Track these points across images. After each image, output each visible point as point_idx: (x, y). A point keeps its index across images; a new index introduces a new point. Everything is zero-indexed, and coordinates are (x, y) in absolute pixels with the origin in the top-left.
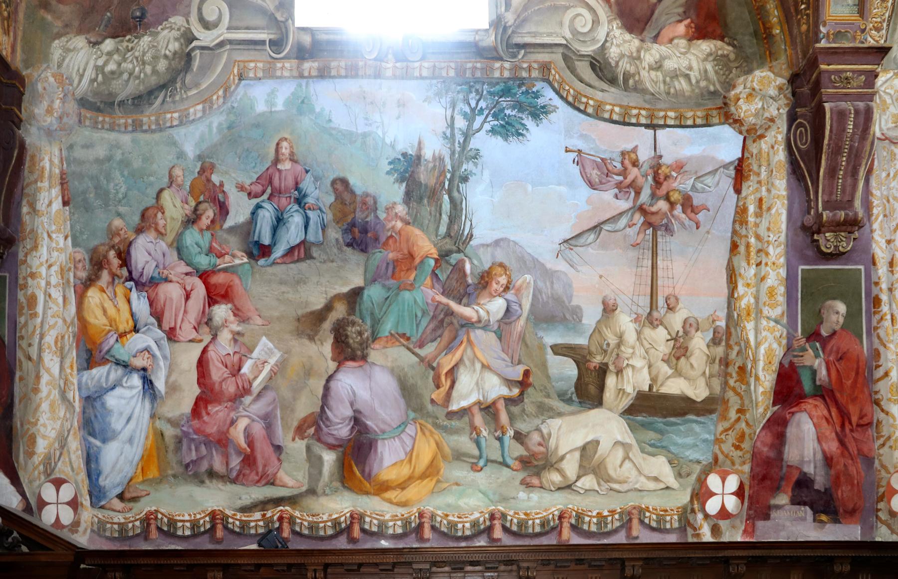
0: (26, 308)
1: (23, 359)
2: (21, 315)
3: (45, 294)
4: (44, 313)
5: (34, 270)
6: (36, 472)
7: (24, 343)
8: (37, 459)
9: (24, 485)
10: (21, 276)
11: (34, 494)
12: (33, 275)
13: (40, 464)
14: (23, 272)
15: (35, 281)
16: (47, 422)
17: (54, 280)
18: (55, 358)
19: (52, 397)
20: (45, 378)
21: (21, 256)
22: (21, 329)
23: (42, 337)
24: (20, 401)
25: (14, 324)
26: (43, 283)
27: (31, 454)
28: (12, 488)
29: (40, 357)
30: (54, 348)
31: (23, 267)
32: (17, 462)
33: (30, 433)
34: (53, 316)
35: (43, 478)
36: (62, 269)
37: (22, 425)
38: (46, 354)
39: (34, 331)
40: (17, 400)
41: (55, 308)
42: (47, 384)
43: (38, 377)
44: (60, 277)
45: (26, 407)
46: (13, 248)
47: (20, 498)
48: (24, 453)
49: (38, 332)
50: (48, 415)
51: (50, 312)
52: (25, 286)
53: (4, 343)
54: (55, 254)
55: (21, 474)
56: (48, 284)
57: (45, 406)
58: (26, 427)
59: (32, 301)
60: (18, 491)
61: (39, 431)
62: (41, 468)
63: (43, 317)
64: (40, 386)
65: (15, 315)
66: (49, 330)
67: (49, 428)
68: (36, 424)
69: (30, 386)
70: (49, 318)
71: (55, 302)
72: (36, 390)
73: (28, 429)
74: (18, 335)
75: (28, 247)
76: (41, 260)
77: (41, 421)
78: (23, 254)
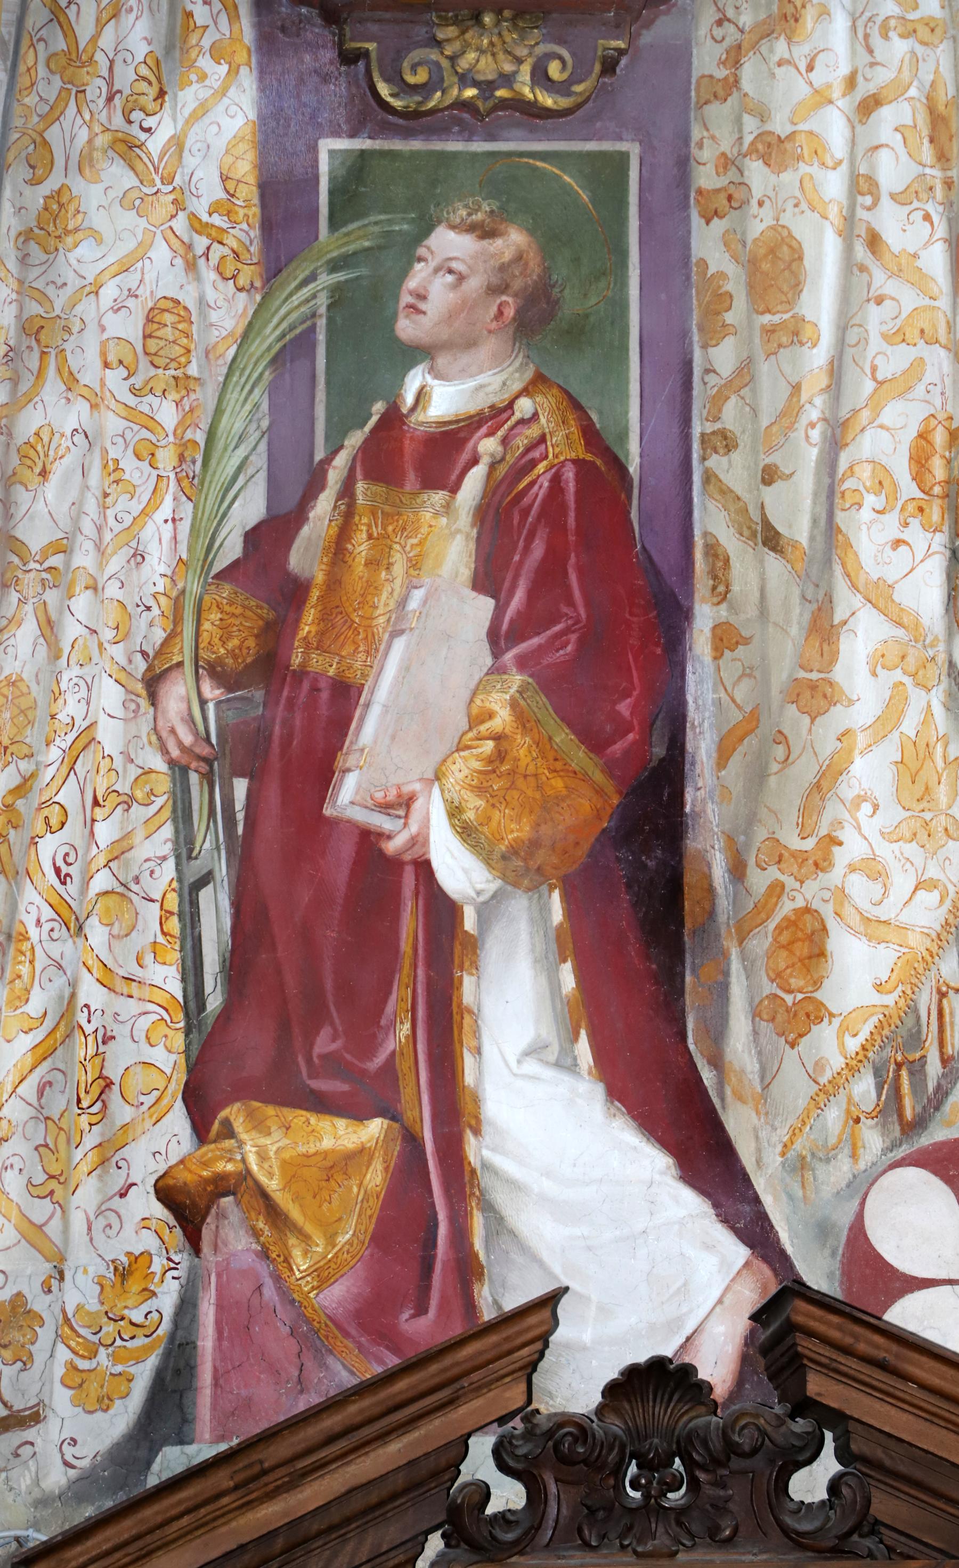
0: (740, 303)
1: (729, 541)
2: (715, 332)
3: (847, 231)
4: (844, 325)
5: (780, 125)
6: (833, 1116)
7: (734, 470)
8: (830, 1046)
9: (760, 1184)
10: (707, 154)
11: (823, 1230)
12: (774, 150)
13: (852, 1069)
14: (715, 135)
15: (788, 177)
16: (885, 851)
17: (892, 170)
18: (917, 535)
19: (909, 726)
20: (864, 635)
21: (706, 60)
22: (718, 400)
23: (838, 435)
24: (723, 756)
25: (676, 383)
26: (834, 186)
27: (797, 1017)
28: (688, 1205)
29: (831, 533)
30: (909, 489)
31: (719, 113)
32: (717, 1062)
33: (786, 908)
34: (897, 337)
35: (873, 1141)
36: (937, 120)
37: (738, 870)
38: (866, 514)
39: (790, 412)
40: (702, 745)
41: (909, 299)
42: (879, 662)
43: (824, 630)
44: (927, 153)
45: (758, 776)
46: (660, 30)
47: (739, 1253)
48: (756, 1014)
49: (814, 414)
50: (892, 814)
51: (876, 319)
52: (734, 199)
53: (620, 467)
54: (899, 47)
55: (739, 1123)
56: (862, 185)
57: (870, 772)
58: (759, 880)
59: (776, 269)
60: (726, 1219)
61: (841, 894)
62: (864, 1088)
63: (841, 343)
64: (838, 674)
65: (685, 335)
66: (876, 404)
67: (902, 883)
68: (822, 864)
69: (782, 672)
70: (875, 343)
71: (907, 268)
72: (816, 695)
73: (777, 889)
74: (697, 429)
75: (746, 19)
76: (818, 77)
77: (852, 848)
78: (719, 51)
